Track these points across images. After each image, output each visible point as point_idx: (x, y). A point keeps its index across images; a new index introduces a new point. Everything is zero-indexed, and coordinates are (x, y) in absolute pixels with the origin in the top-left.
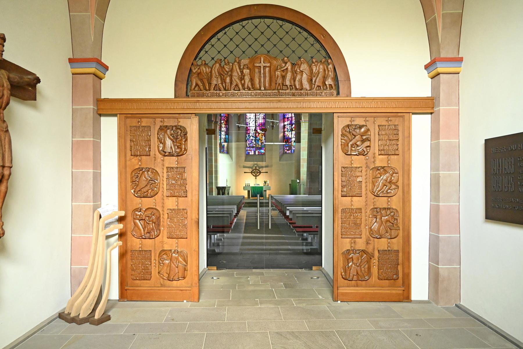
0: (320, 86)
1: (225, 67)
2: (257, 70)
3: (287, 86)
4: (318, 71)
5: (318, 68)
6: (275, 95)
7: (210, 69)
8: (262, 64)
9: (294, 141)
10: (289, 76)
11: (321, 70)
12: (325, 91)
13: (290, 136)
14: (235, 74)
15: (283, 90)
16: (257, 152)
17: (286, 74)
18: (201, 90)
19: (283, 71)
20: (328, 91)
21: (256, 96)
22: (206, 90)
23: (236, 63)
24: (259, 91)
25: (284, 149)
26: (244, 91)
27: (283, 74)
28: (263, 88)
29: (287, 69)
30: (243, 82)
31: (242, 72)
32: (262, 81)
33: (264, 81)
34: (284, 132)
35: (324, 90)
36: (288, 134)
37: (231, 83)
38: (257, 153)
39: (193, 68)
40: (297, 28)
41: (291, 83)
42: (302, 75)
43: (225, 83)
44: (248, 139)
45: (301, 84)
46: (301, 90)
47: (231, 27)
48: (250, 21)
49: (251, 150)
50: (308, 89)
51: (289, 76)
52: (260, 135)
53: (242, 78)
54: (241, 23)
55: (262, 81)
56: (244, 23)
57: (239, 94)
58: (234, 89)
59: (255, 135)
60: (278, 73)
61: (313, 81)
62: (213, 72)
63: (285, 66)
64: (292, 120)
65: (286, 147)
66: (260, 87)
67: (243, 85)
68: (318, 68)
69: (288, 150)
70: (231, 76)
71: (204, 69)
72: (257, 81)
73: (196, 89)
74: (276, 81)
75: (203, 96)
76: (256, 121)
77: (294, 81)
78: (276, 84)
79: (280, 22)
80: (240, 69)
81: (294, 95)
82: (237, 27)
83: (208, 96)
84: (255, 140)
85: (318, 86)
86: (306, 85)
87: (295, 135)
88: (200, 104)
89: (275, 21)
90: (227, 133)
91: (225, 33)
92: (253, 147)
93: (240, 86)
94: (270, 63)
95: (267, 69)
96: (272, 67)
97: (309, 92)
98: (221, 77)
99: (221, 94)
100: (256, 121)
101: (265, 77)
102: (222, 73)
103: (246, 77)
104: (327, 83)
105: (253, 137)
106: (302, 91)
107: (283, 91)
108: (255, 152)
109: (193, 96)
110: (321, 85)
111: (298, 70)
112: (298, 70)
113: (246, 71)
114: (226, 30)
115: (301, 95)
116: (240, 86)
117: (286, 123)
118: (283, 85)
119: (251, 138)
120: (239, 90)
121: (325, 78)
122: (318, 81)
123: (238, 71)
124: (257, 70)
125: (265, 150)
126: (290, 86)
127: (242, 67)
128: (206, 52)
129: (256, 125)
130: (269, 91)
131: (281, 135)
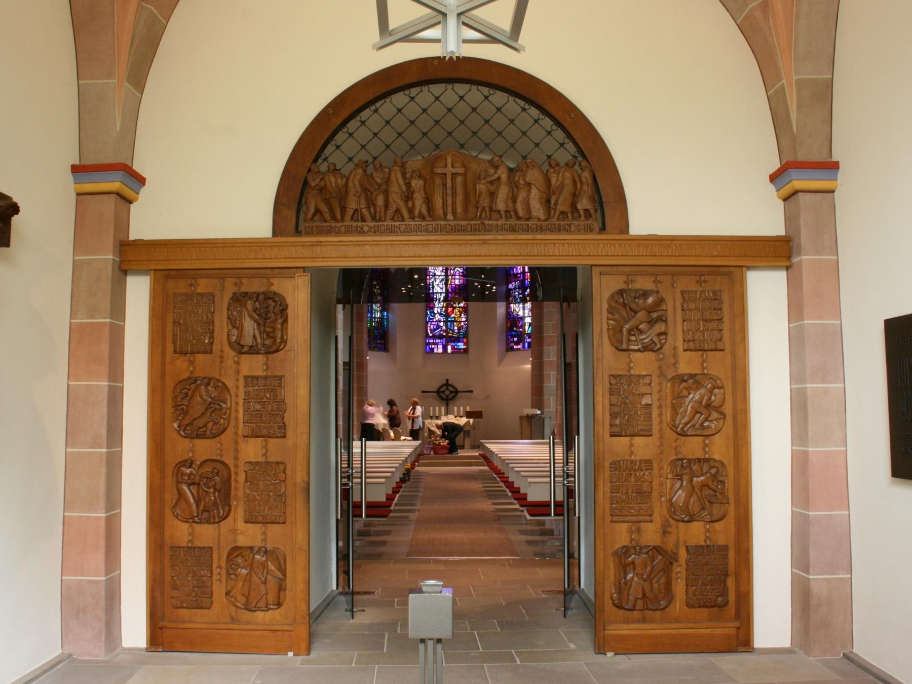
0: (566, 213)
1: (375, 175)
2: (438, 181)
3: (499, 211)
4: (562, 183)
5: (560, 178)
6: (475, 230)
7: (344, 180)
8: (449, 170)
9: (530, 325)
10: (503, 193)
11: (567, 182)
12: (576, 223)
13: (521, 314)
14: (394, 188)
15: (490, 219)
16: (449, 348)
17: (498, 188)
18: (325, 221)
19: (491, 182)
20: (582, 223)
21: (437, 231)
22: (336, 221)
23: (396, 168)
24: (443, 223)
25: (507, 340)
26: (413, 223)
27: (492, 188)
28: (450, 217)
29: (499, 179)
30: (410, 204)
31: (408, 185)
32: (450, 201)
33: (454, 203)
35: (574, 218)
36: (519, 309)
37: (387, 206)
39: (310, 179)
40: (517, 100)
41: (507, 205)
42: (529, 191)
43: (375, 206)
44: (431, 320)
45: (528, 209)
46: (528, 220)
47: (388, 100)
48: (425, 89)
49: (437, 344)
50: (542, 217)
51: (503, 193)
52: (456, 310)
53: (408, 197)
54: (407, 92)
55: (450, 201)
56: (414, 91)
57: (403, 227)
58: (392, 219)
59: (446, 311)
60: (481, 187)
61: (553, 202)
62: (351, 185)
63: (495, 173)
64: (524, 279)
65: (513, 337)
66: (445, 214)
67: (411, 211)
68: (560, 178)
69: (517, 343)
70: (386, 193)
71: (333, 180)
72: (438, 202)
73: (316, 218)
74: (477, 202)
75: (329, 232)
76: (447, 281)
77: (514, 201)
78: (477, 208)
79: (485, 90)
80: (404, 178)
81: (513, 230)
82: (400, 99)
83: (338, 233)
84: (446, 322)
85: (562, 213)
86: (538, 210)
87: (532, 310)
88: (324, 248)
89: (474, 88)
91: (376, 111)
92: (440, 337)
93: (405, 213)
94: (465, 166)
95: (459, 179)
96: (469, 175)
97: (544, 223)
98: (366, 194)
99: (366, 229)
101: (454, 194)
102: (369, 187)
103: (416, 195)
104: (579, 207)
105: (440, 314)
106: (530, 223)
107: (490, 222)
108: (445, 348)
109: (309, 233)
110: (566, 209)
111: (522, 182)
112: (522, 182)
113: (417, 184)
114: (378, 104)
115: (527, 230)
116: (405, 213)
117: (510, 286)
118: (491, 209)
119: (438, 317)
120: (403, 220)
121: (575, 196)
122: (562, 203)
123: (401, 182)
124: (438, 181)
125: (466, 344)
126: (506, 212)
127: (408, 176)
128: (338, 147)
129: (447, 290)
130: (464, 223)
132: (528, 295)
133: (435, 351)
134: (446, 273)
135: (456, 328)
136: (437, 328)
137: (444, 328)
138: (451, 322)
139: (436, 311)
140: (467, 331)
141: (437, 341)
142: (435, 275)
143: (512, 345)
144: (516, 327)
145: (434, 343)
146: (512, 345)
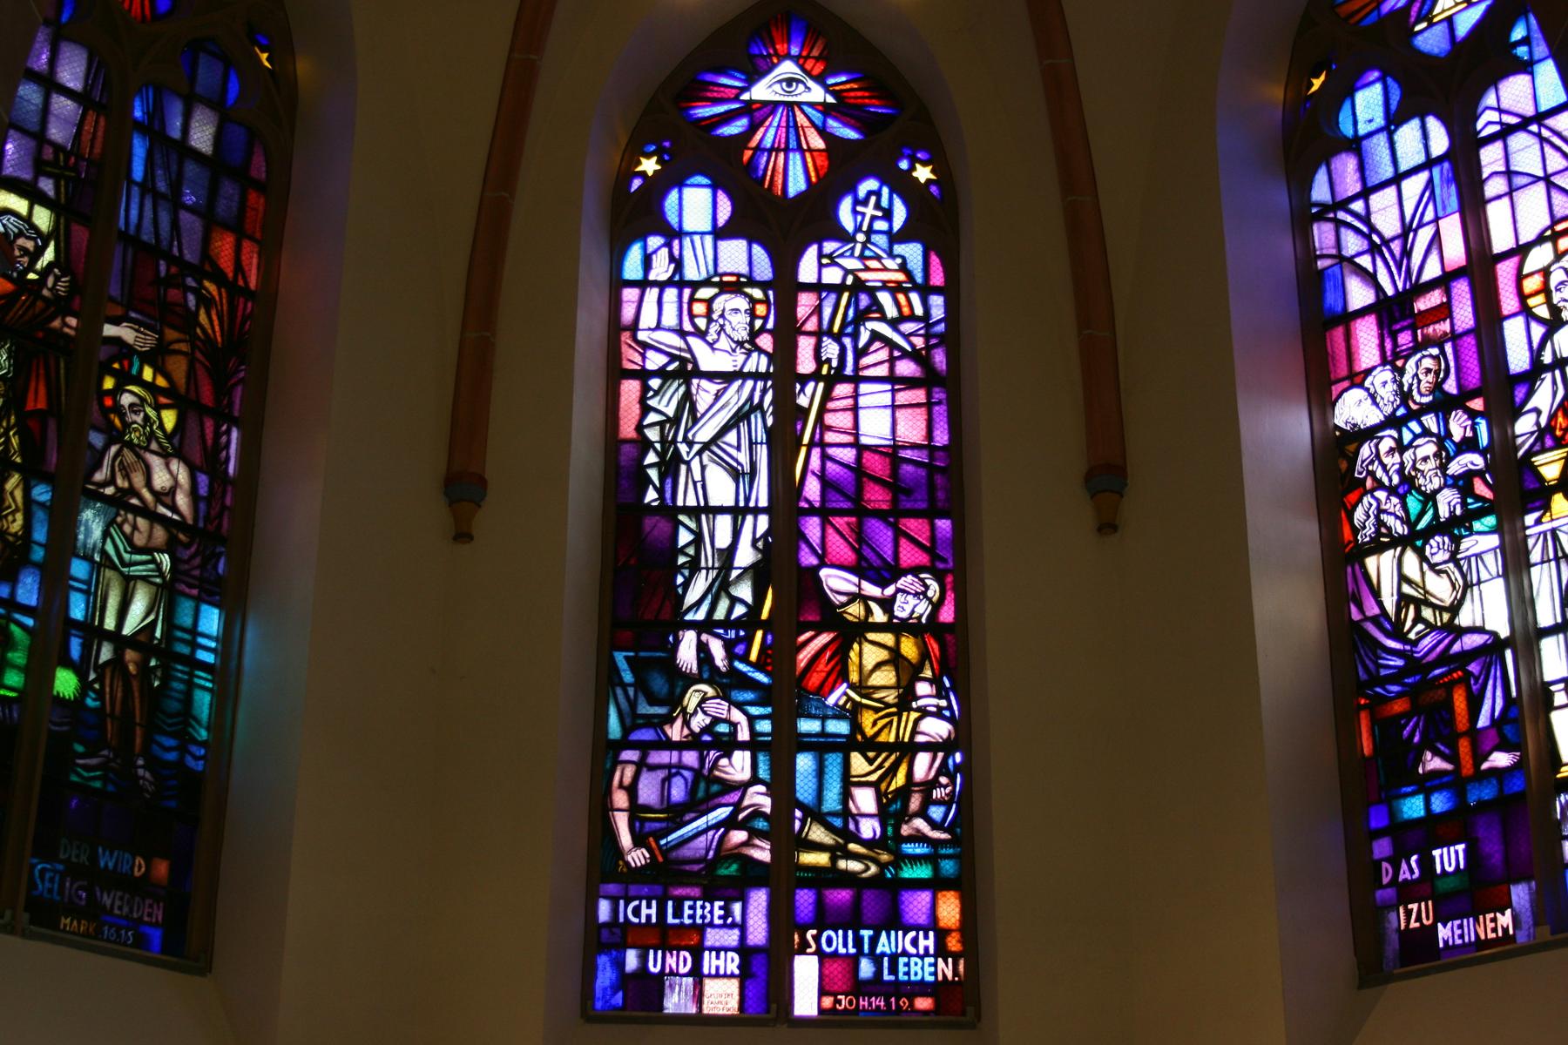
16: (806, 970)
25: (1363, 874)
34: (1343, 560)
38: (806, 1002)
44: (645, 735)
59: (777, 657)
76: (788, 416)
84: (778, 750)
90: (213, 553)
92: (725, 879)
100: (788, 416)
105: (728, 684)
117: (1353, 409)
131: (1285, 608)
132: (1547, 437)
133: (676, 1001)
134: (784, 355)
135: (865, 800)
136: (697, 804)
137: (758, 797)
138: (822, 746)
139: (687, 654)
140: (964, 802)
141: (697, 910)
142: (685, 371)
143: (1417, 914)
144: (1441, 733)
145: (664, 937)
146: (1417, 914)
